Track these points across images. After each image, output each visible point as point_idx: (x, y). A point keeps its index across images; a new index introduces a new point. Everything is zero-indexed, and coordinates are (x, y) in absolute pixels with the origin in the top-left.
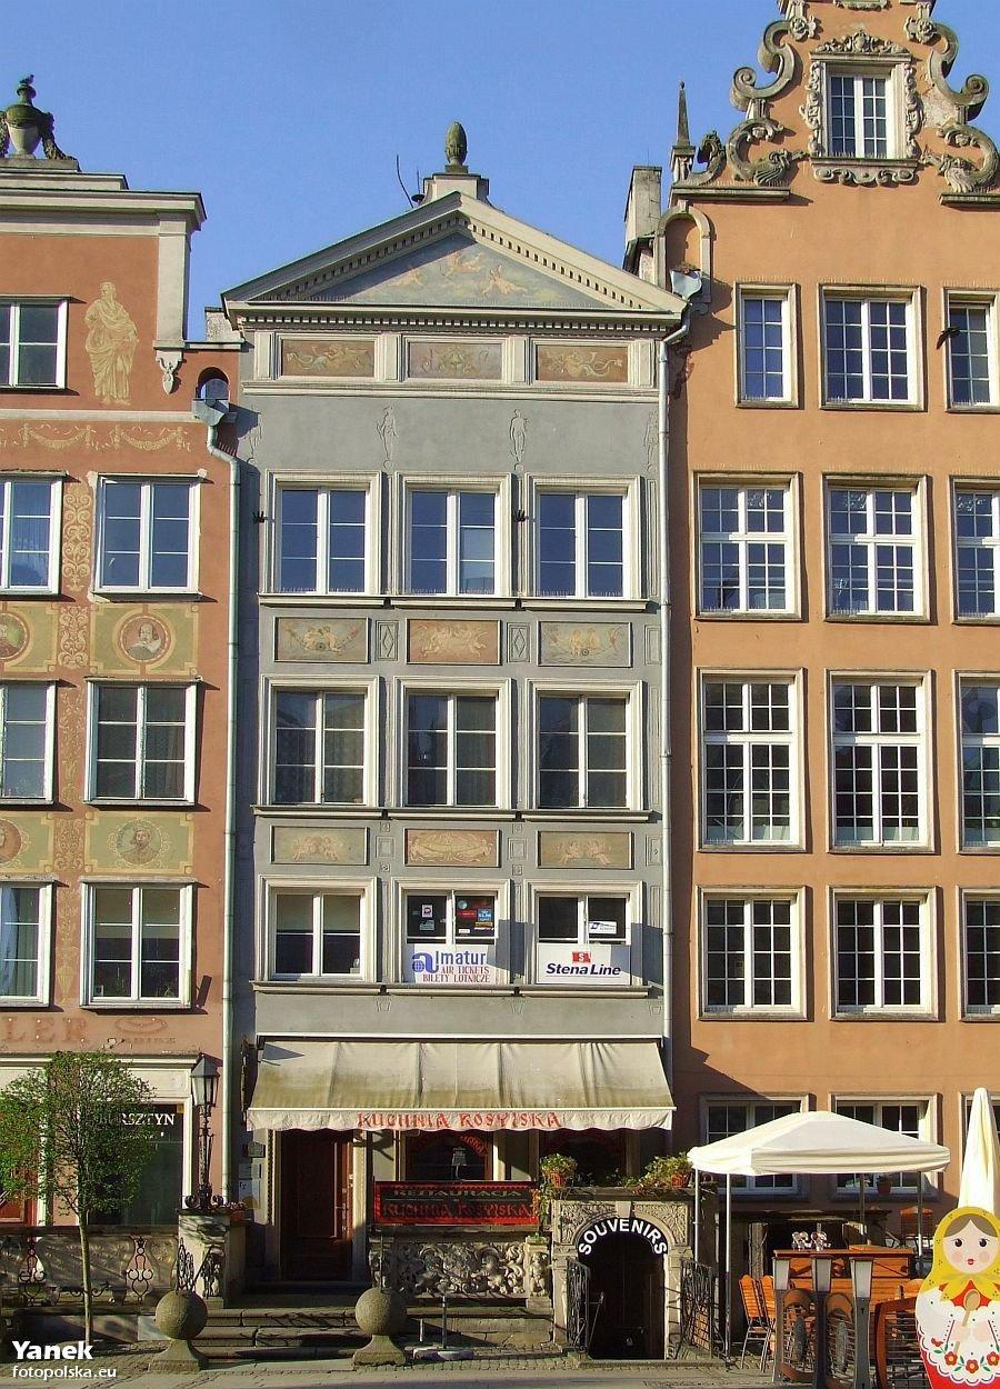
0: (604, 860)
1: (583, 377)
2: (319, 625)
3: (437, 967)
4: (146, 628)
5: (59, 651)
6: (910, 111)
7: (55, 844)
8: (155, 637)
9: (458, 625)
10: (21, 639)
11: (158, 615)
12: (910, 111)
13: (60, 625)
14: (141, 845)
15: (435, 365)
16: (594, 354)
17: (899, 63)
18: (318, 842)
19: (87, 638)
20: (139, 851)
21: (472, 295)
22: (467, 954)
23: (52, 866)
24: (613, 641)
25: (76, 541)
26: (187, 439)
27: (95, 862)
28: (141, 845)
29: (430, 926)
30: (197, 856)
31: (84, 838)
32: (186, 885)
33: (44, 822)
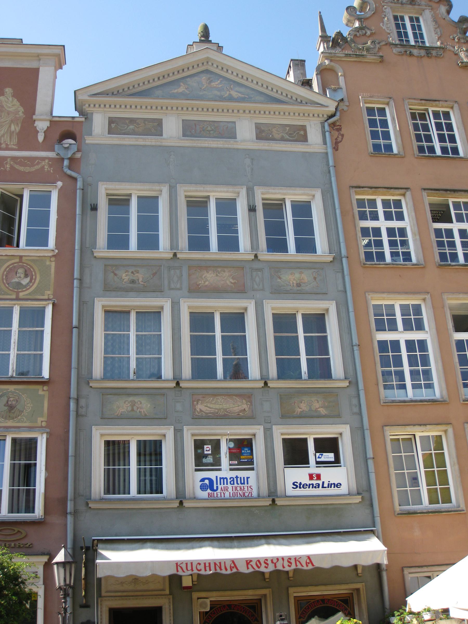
0: (323, 411)
1: (283, 139)
3: (217, 487)
4: (21, 271)
6: (436, 28)
8: (26, 276)
9: (219, 270)
11: (29, 263)
12: (436, 28)
14: (11, 408)
16: (288, 128)
17: (426, 9)
18: (133, 404)
20: (10, 411)
22: (237, 477)
24: (315, 278)
26: (50, 166)
28: (11, 408)
29: (210, 460)
30: (50, 414)
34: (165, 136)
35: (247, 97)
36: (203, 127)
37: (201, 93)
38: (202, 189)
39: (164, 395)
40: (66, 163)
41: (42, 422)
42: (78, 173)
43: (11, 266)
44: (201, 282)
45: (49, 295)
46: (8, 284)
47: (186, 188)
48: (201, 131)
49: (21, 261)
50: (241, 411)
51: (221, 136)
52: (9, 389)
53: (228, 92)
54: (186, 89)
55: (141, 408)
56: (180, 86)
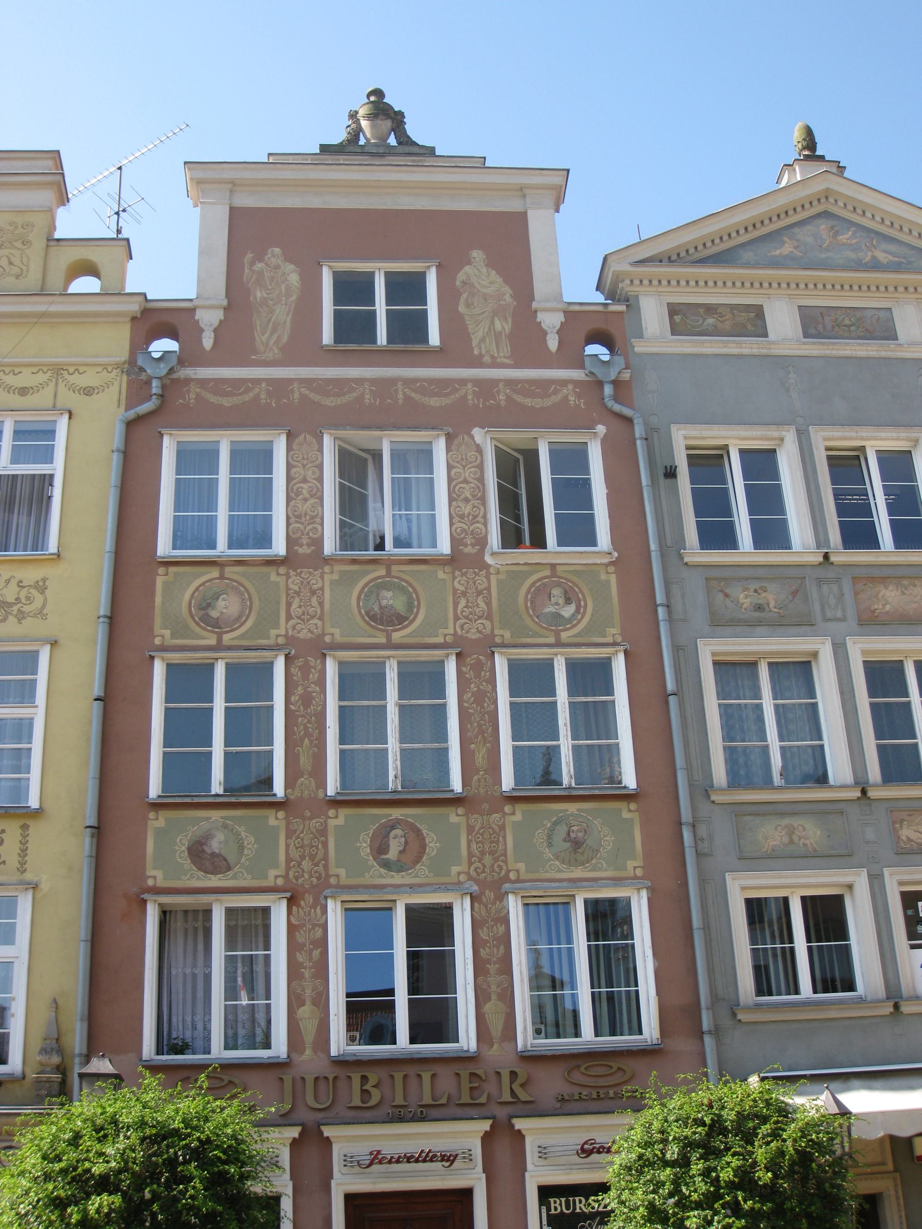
4: (556, 592)
5: (457, 618)
7: (469, 846)
8: (568, 601)
9: (906, 582)
10: (410, 606)
13: (455, 590)
14: (577, 844)
18: (791, 831)
19: (489, 604)
20: (575, 852)
23: (468, 873)
25: (467, 500)
26: (579, 396)
27: (521, 866)
28: (577, 844)
30: (647, 855)
31: (504, 838)
33: (453, 819)
34: (772, 336)
36: (836, 319)
37: (823, 256)
38: (854, 434)
39: (842, 812)
40: (608, 390)
41: (635, 868)
42: (631, 407)
43: (538, 584)
45: (614, 635)
46: (538, 617)
47: (827, 434)
48: (833, 327)
49: (554, 573)
51: (869, 335)
52: (567, 810)
53: (869, 253)
54: (795, 248)
55: (806, 838)
56: (783, 243)
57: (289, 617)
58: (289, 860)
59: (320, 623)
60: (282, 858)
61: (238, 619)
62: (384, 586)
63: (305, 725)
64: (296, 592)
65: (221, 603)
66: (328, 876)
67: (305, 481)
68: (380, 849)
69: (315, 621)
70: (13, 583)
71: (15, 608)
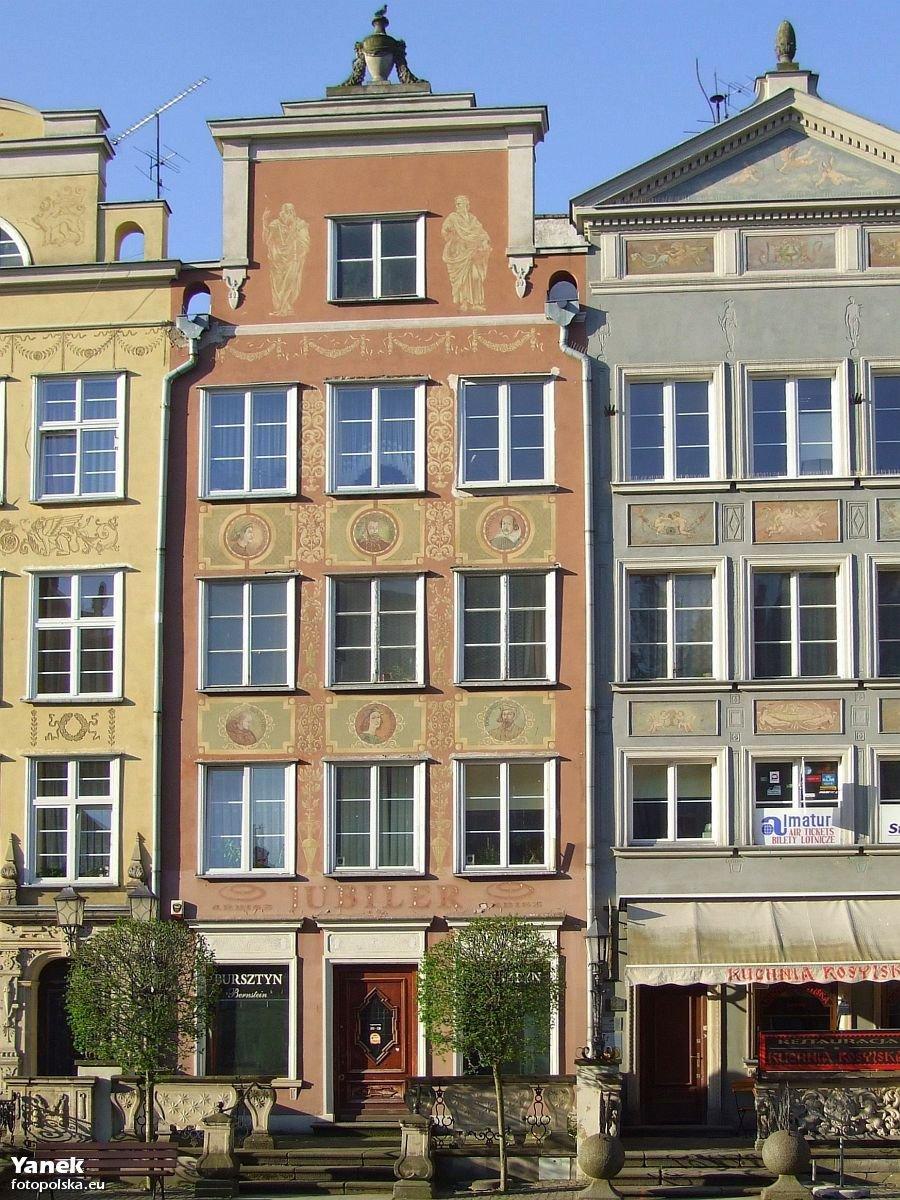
2: (670, 510)
4: (507, 520)
5: (427, 544)
7: (427, 725)
8: (516, 527)
9: (800, 505)
13: (427, 520)
14: (507, 723)
15: (771, 258)
18: (673, 715)
19: (452, 531)
21: (806, 188)
22: (813, 816)
25: (440, 441)
26: (539, 339)
27: (464, 740)
28: (507, 723)
29: (778, 791)
32: (550, 759)
33: (417, 704)
35: (857, 180)
36: (781, 248)
44: (772, 528)
50: (823, 724)
55: (683, 722)
57: (299, 545)
58: (297, 735)
59: (322, 550)
60: (293, 732)
61: (260, 548)
62: (374, 518)
63: (310, 632)
64: (304, 525)
65: (248, 535)
66: (325, 747)
67: (312, 427)
68: (363, 726)
69: (317, 548)
70: (93, 521)
71: (96, 542)
